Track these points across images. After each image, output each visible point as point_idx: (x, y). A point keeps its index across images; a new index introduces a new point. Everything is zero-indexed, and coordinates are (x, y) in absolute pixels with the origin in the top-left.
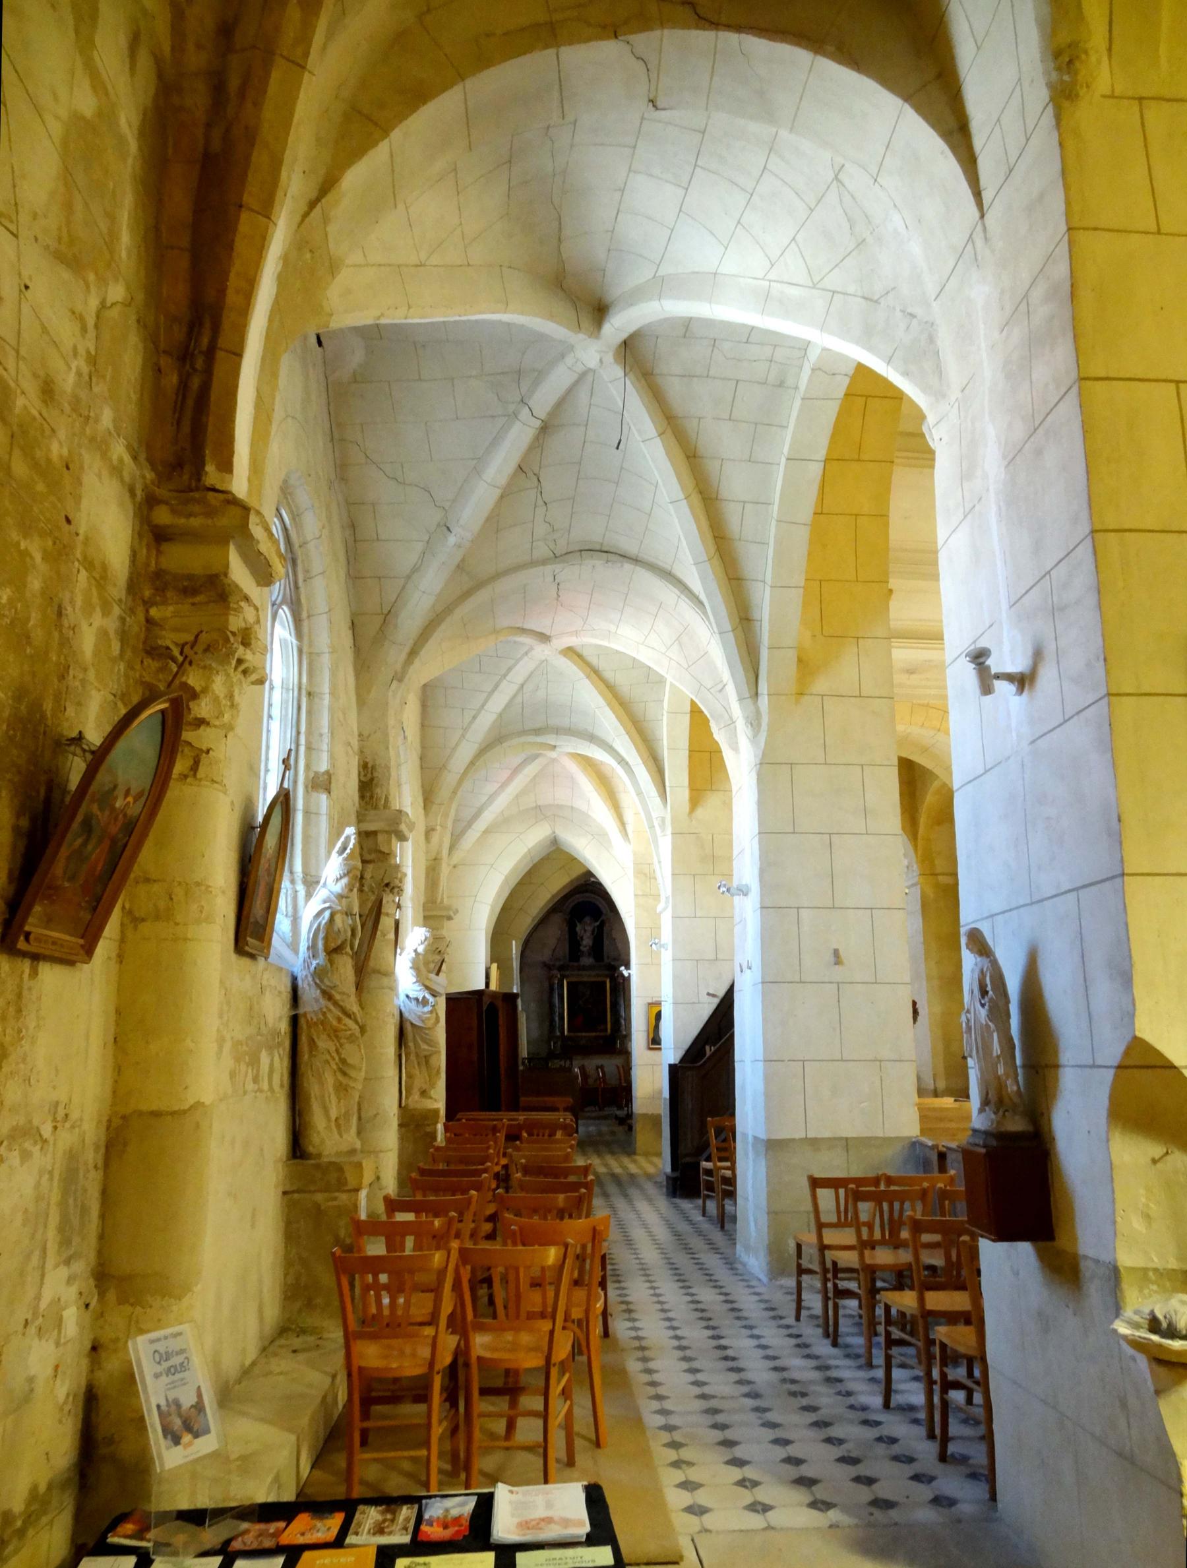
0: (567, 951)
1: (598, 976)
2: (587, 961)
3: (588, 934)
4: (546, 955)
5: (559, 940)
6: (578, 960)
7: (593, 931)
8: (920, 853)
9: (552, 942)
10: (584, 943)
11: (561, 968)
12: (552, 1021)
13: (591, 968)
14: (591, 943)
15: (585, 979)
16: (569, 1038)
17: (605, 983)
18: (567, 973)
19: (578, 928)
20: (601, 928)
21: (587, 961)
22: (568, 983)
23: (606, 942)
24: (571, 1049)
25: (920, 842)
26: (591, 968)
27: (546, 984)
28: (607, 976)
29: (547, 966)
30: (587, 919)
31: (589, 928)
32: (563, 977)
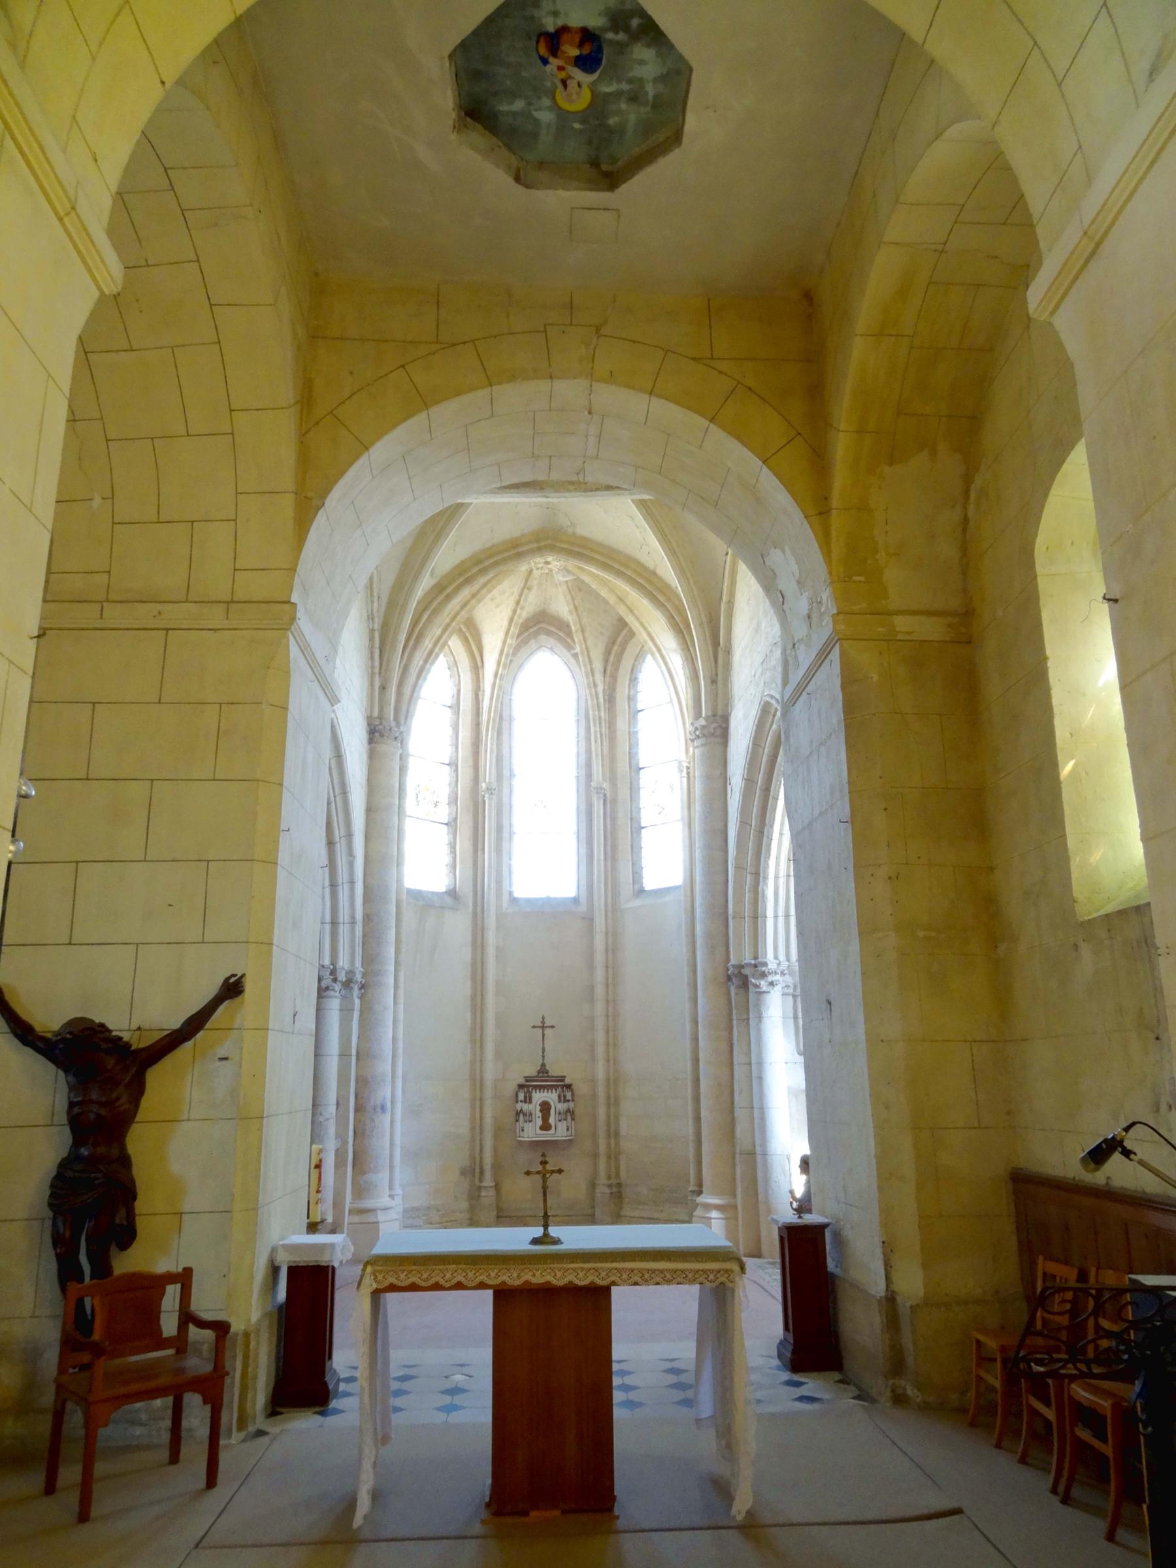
8: (837, 549)
25: (837, 521)
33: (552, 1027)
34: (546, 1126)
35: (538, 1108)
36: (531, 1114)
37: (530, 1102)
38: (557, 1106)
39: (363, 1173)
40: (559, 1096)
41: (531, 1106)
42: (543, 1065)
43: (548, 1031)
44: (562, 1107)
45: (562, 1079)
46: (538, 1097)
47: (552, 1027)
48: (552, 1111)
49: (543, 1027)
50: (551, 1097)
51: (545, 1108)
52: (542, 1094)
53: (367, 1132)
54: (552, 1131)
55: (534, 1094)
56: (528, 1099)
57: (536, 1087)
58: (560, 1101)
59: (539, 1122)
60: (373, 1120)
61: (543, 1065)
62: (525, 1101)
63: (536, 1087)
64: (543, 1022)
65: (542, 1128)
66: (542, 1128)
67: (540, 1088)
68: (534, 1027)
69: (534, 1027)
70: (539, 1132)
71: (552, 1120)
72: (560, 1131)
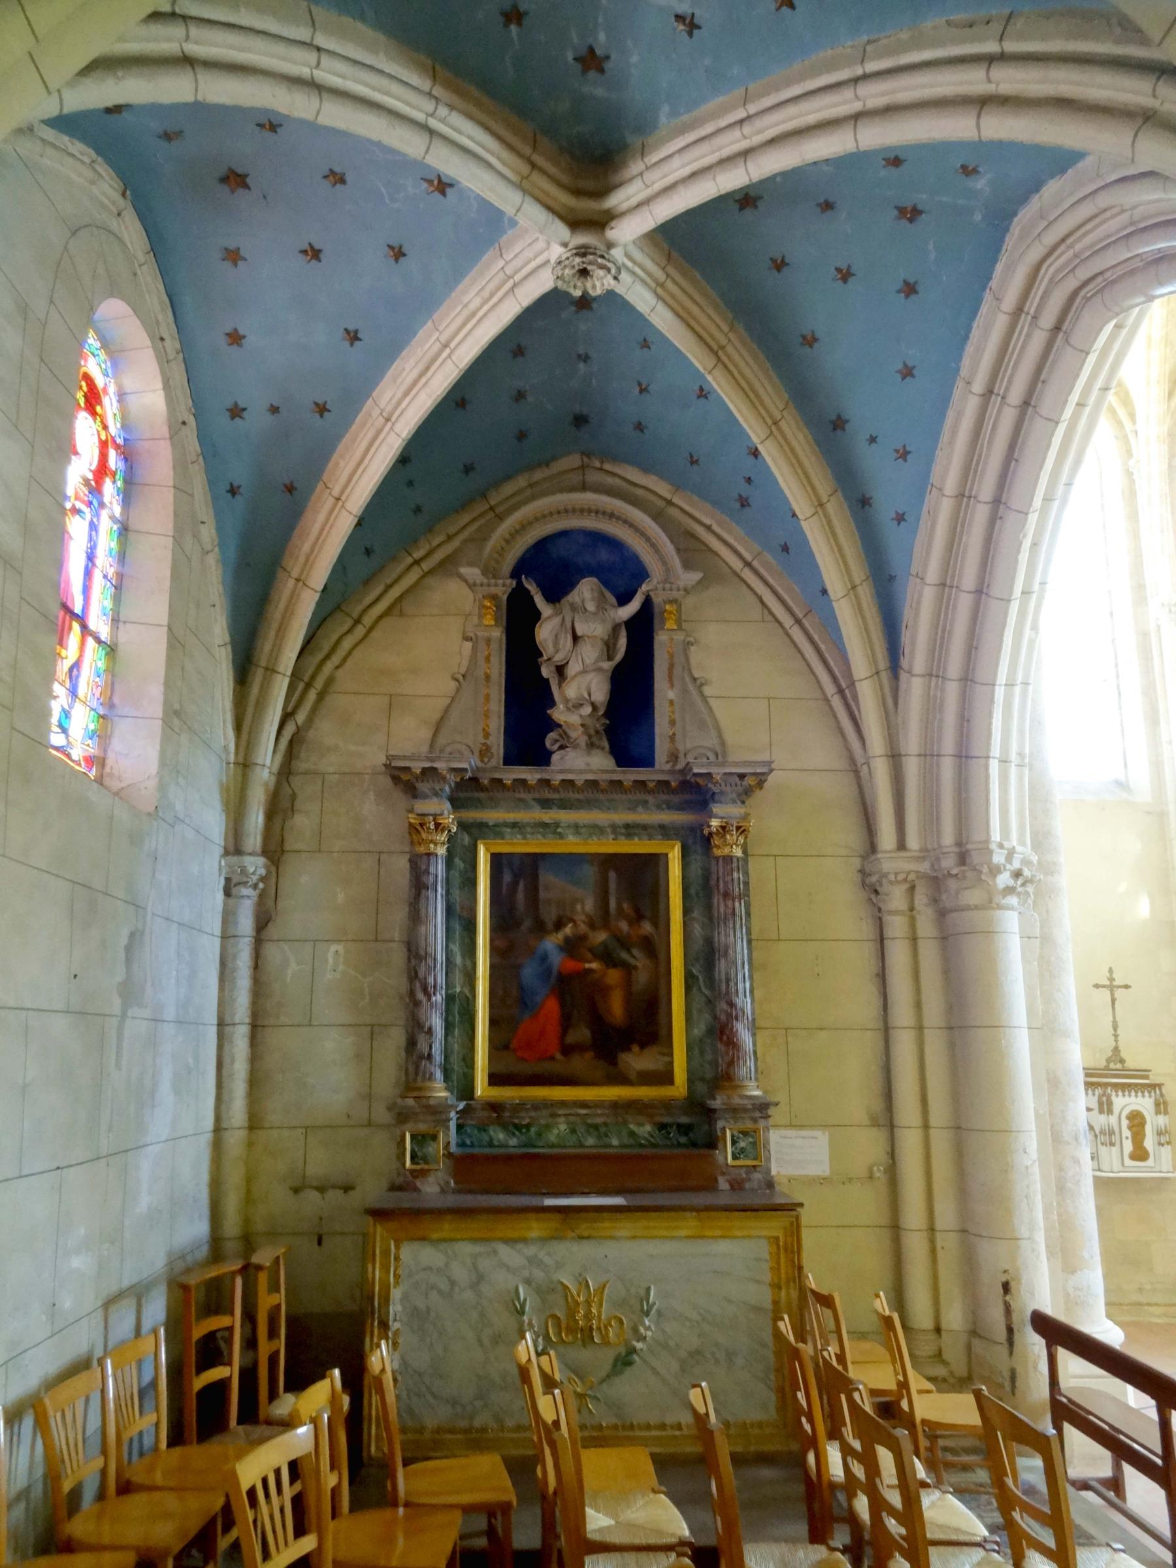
0: (497, 724)
1: (630, 830)
2: (581, 761)
3: (590, 653)
4: (409, 738)
5: (461, 679)
6: (542, 758)
7: (609, 648)
9: (433, 688)
10: (572, 690)
11: (469, 790)
12: (416, 1029)
13: (594, 791)
14: (600, 692)
15: (572, 844)
16: (495, 1107)
17: (653, 864)
18: (492, 816)
19: (544, 633)
20: (642, 629)
21: (581, 761)
22: (497, 861)
23: (664, 693)
24: (502, 1177)
26: (594, 791)
27: (400, 865)
28: (665, 831)
29: (405, 780)
30: (586, 591)
31: (594, 629)
32: (476, 830)
33: (1127, 987)
34: (1140, 1154)
35: (1125, 1123)
36: (1111, 1133)
37: (1110, 1112)
38: (1153, 1122)
39: (1073, 1272)
40: (1157, 1104)
41: (1113, 1120)
42: (1116, 1049)
43: (1119, 993)
44: (1162, 1120)
45: (1144, 1073)
46: (1123, 1103)
47: (1127, 987)
48: (1149, 1129)
49: (1112, 988)
50: (1144, 1103)
51: (1137, 1121)
52: (1127, 1100)
53: (1069, 1185)
54: (1150, 1162)
55: (1114, 1098)
56: (1105, 1107)
57: (1116, 1086)
58: (1158, 1112)
59: (1128, 1146)
60: (1077, 1161)
61: (1116, 1049)
62: (1101, 1111)
63: (1116, 1086)
64: (1112, 979)
65: (1133, 1157)
66: (1133, 1157)
67: (1124, 1087)
68: (1097, 986)
69: (1097, 986)
70: (1128, 1162)
71: (1149, 1143)
72: (1161, 1162)
